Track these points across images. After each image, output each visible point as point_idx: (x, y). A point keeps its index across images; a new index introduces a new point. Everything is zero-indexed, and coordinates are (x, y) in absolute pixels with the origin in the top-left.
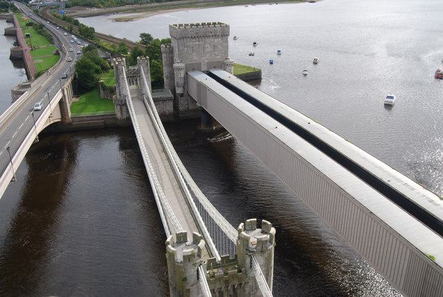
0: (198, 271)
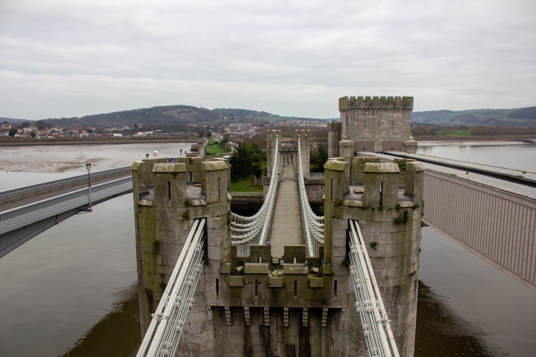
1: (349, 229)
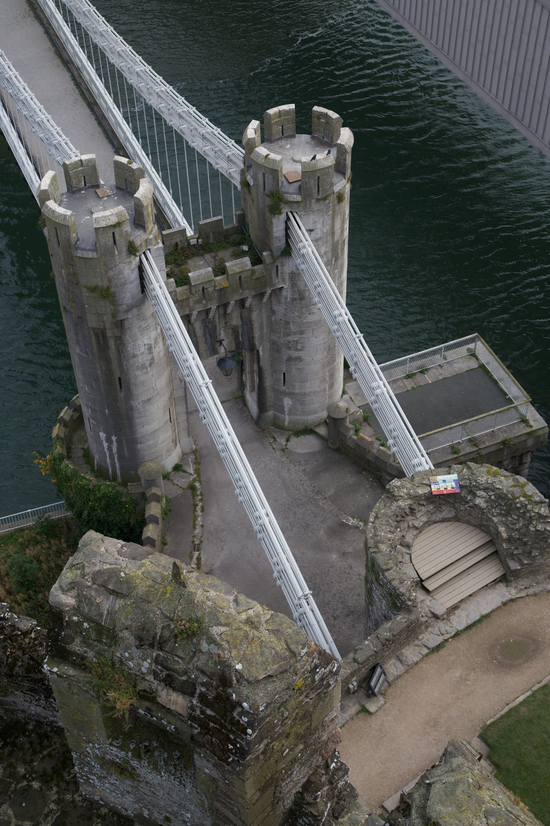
0: (141, 269)
1: (288, 219)
